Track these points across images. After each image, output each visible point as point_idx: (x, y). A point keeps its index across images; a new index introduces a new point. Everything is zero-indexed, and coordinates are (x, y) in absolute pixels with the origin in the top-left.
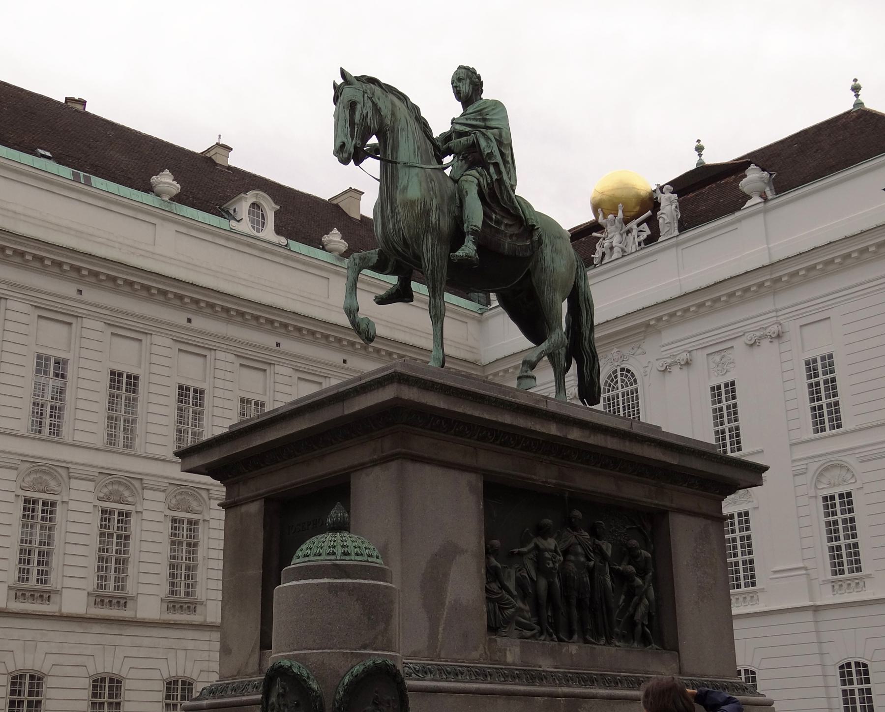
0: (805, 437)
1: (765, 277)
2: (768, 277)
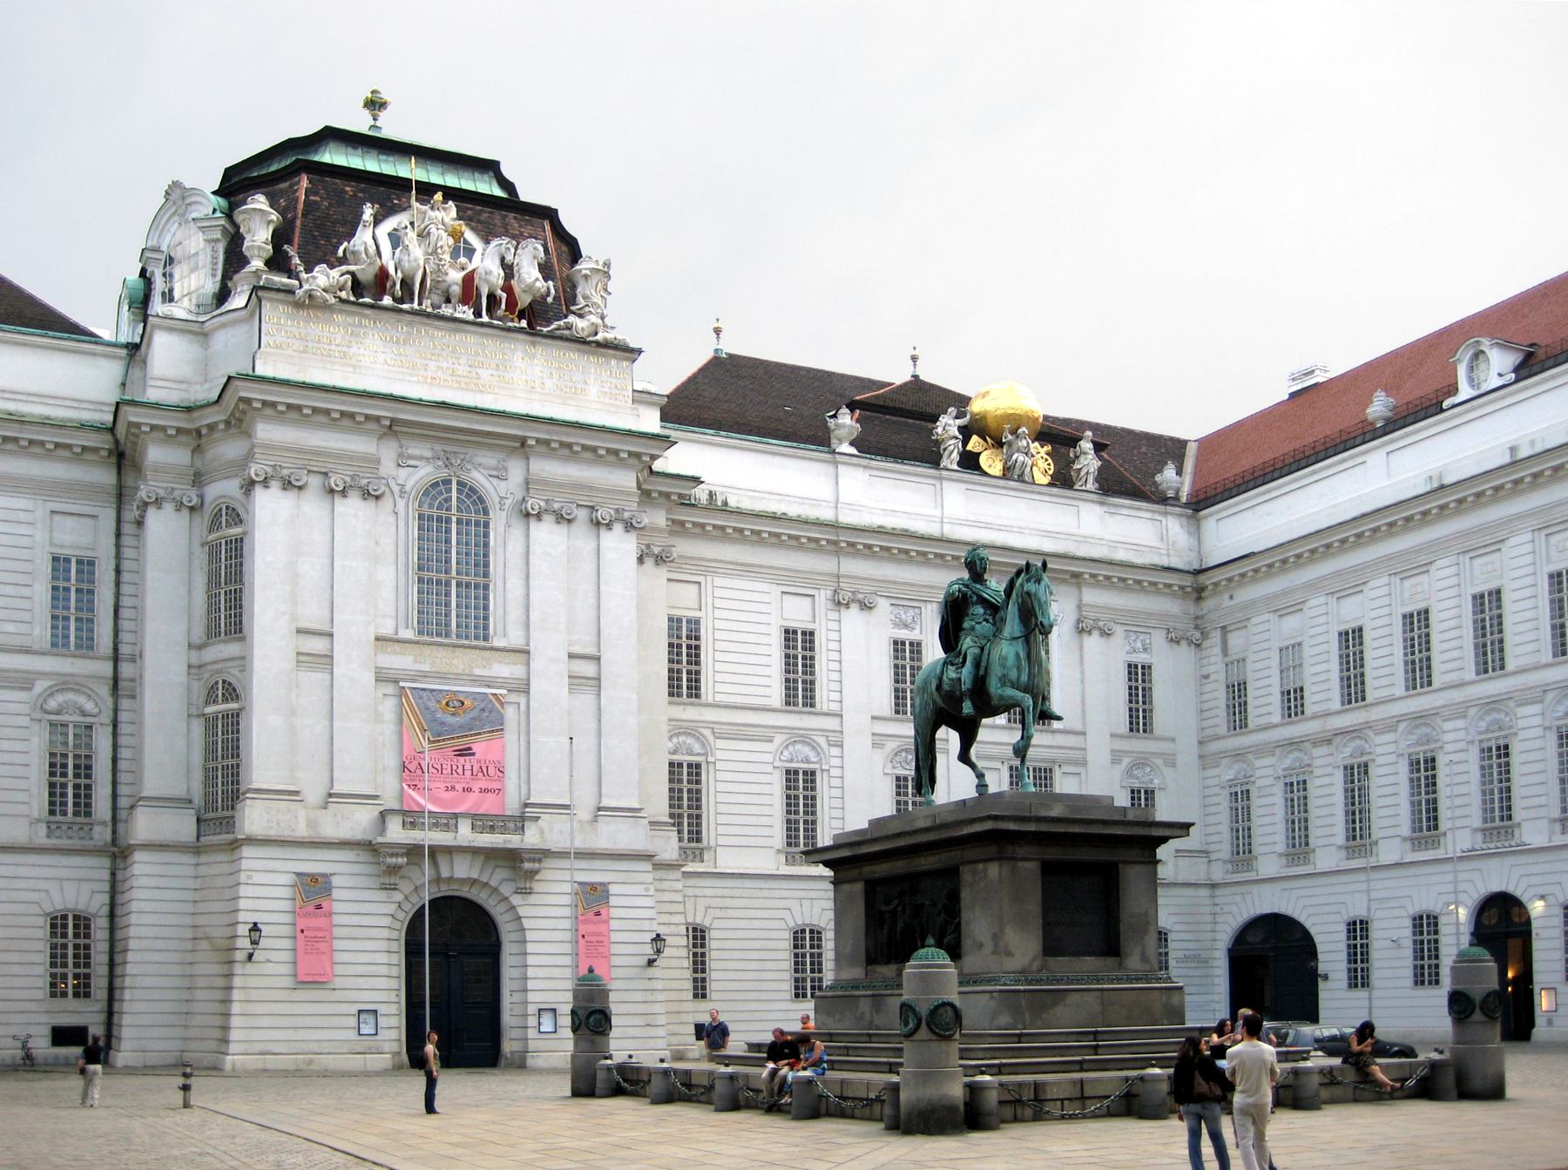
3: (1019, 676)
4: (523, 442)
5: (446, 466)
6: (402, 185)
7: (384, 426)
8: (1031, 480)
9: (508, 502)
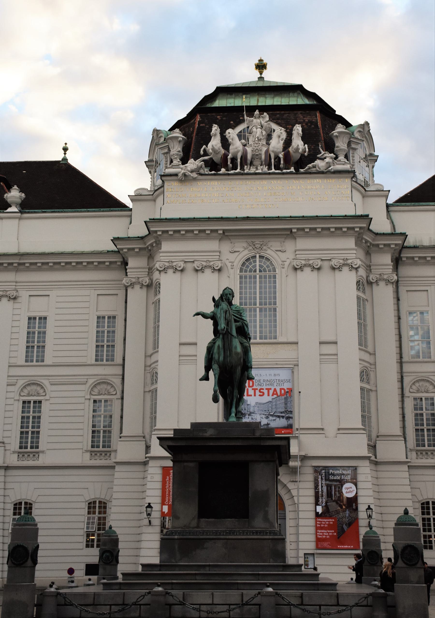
0: (19, 363)
1: (16, 261)
2: (18, 261)
4: (291, 230)
5: (254, 249)
6: (240, 109)
7: (220, 234)
9: (287, 264)
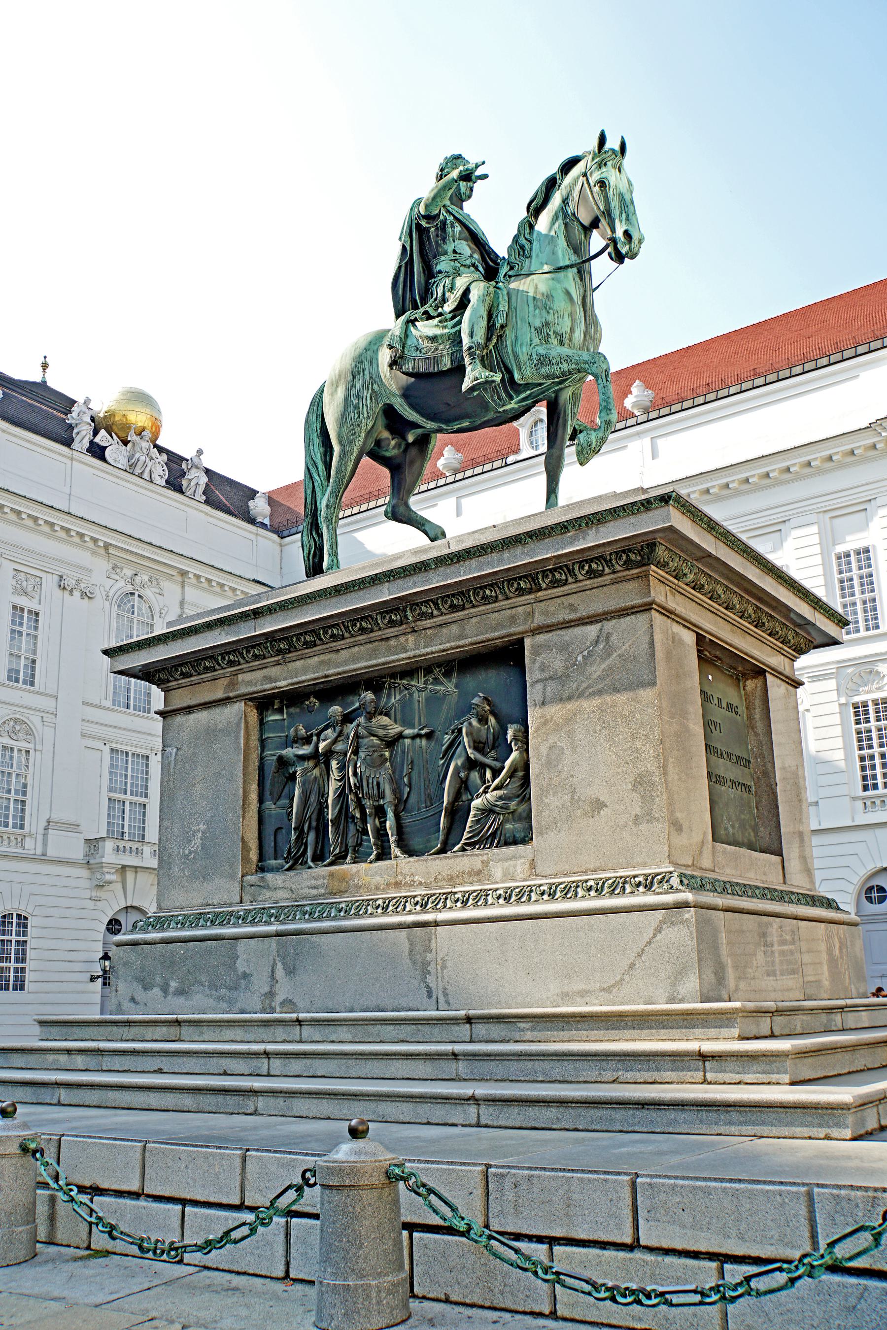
3: (573, 329)
8: (148, 479)
